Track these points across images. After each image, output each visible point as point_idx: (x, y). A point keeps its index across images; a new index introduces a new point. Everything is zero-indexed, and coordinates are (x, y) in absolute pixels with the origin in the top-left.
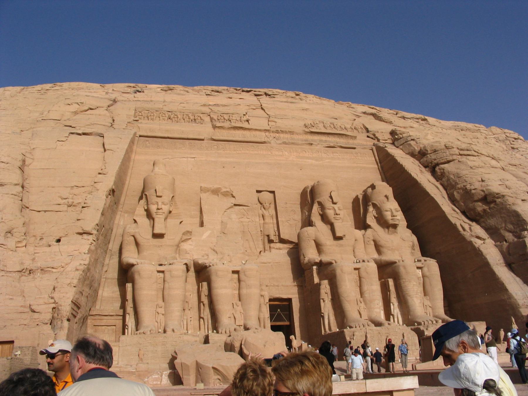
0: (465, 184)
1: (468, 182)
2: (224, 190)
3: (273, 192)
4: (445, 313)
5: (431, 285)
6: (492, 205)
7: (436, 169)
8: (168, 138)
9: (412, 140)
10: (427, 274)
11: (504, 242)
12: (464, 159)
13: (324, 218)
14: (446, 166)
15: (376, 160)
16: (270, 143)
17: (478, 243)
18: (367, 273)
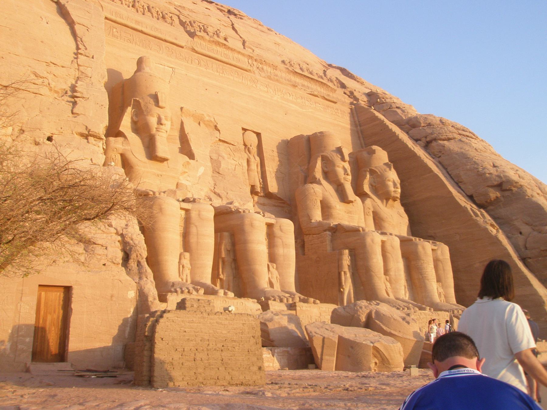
0: (476, 166)
1: (481, 165)
2: (207, 118)
3: (258, 135)
4: (458, 302)
5: (444, 270)
6: (507, 193)
7: (434, 144)
8: (142, 32)
9: (397, 107)
10: (441, 257)
11: (519, 235)
12: (464, 139)
13: (330, 175)
14: (445, 142)
15: (355, 122)
16: (254, 73)
17: (494, 231)
18: (393, 247)
